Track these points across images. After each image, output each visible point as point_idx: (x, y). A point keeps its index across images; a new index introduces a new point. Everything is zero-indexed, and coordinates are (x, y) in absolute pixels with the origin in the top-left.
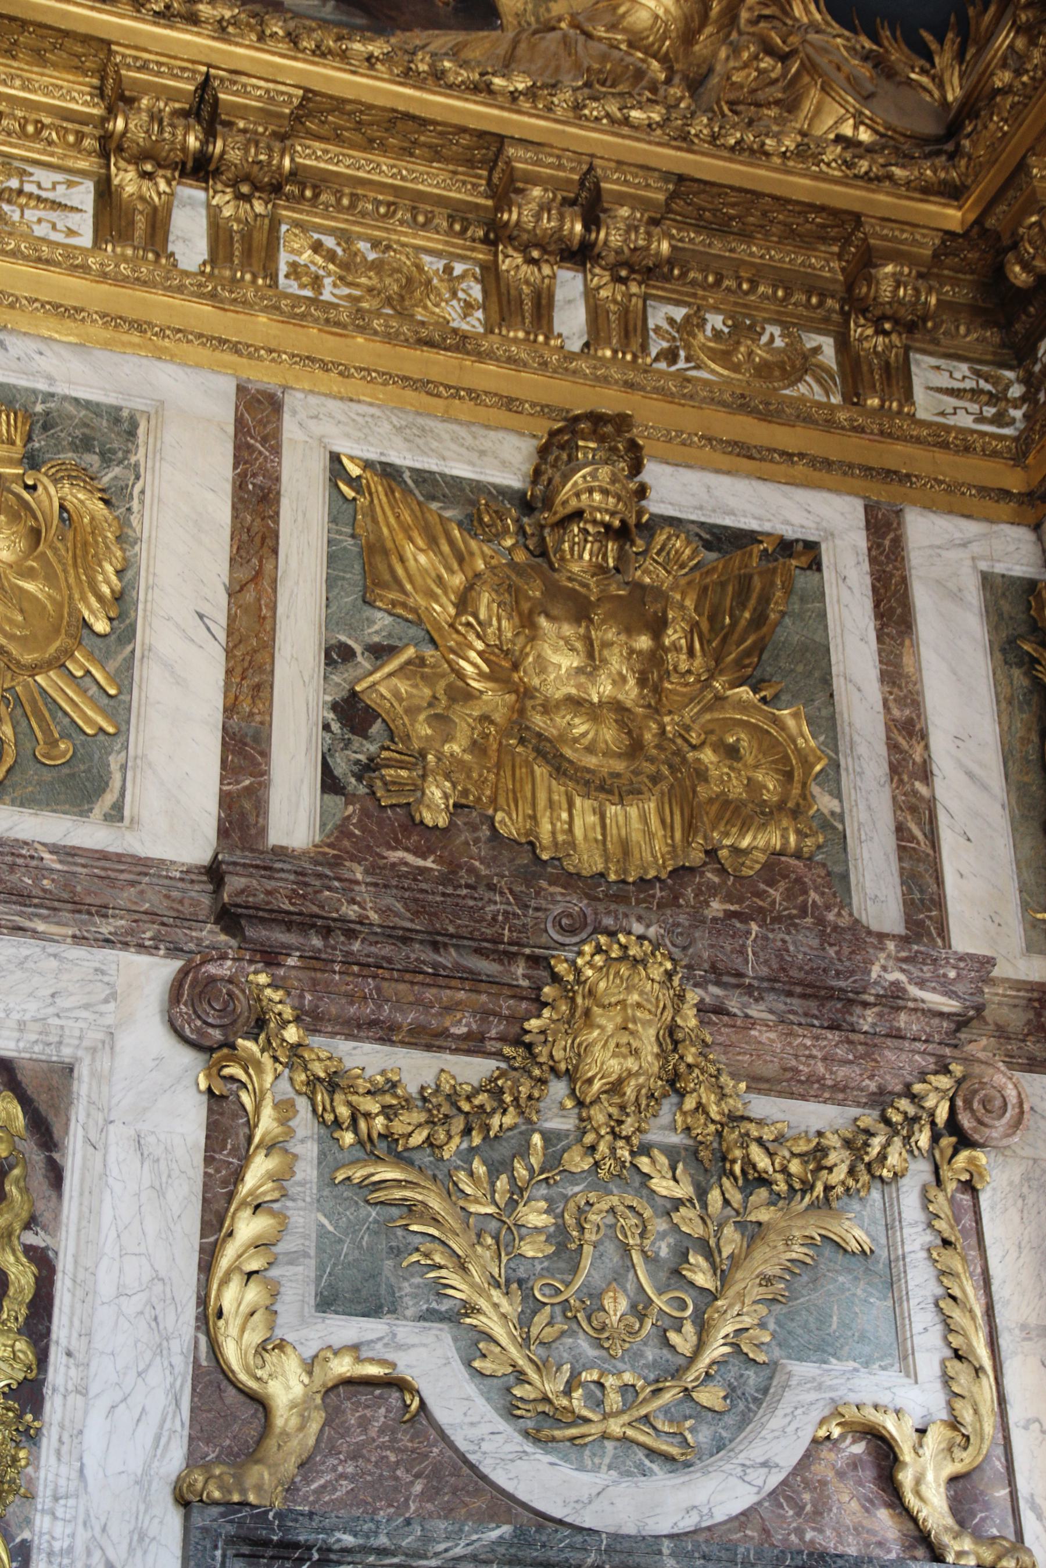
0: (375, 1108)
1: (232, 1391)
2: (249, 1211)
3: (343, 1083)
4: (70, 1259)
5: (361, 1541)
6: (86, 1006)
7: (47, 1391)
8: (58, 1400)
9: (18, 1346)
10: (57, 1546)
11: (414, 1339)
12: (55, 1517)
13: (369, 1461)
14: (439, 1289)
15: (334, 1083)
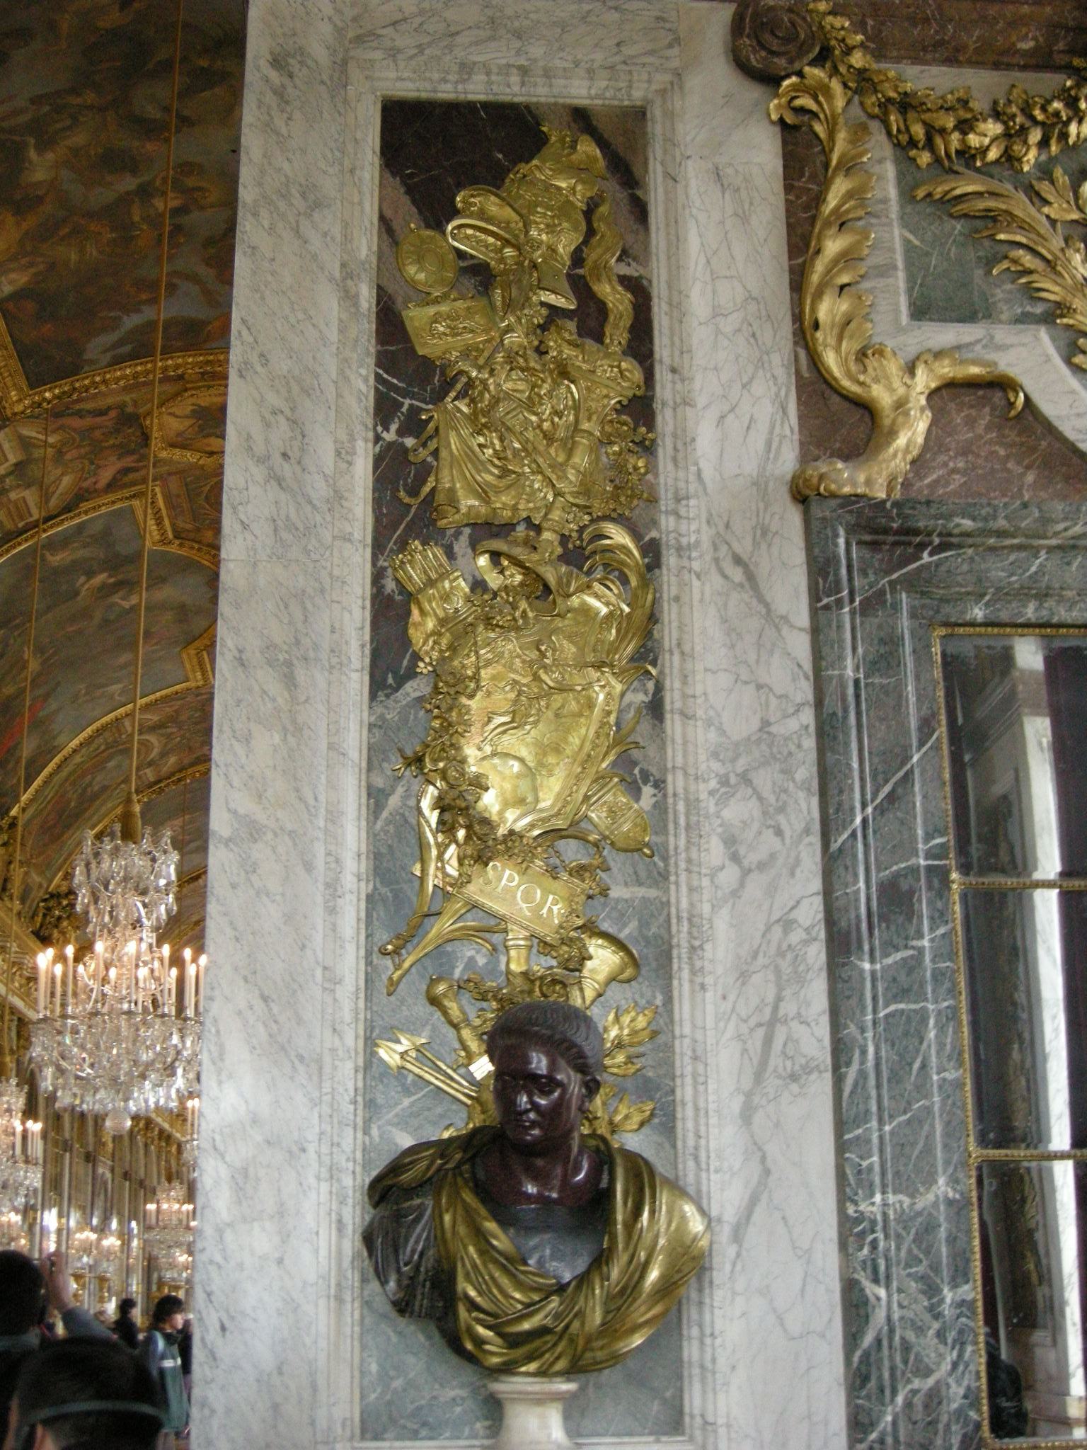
0: (950, 123)
1: (836, 399)
2: (835, 229)
3: (914, 102)
4: (663, 286)
5: (980, 525)
6: (651, 53)
7: (657, 406)
8: (668, 413)
9: (624, 365)
10: (684, 541)
11: (1010, 340)
12: (679, 516)
13: (978, 456)
14: (1031, 293)
15: (907, 104)
